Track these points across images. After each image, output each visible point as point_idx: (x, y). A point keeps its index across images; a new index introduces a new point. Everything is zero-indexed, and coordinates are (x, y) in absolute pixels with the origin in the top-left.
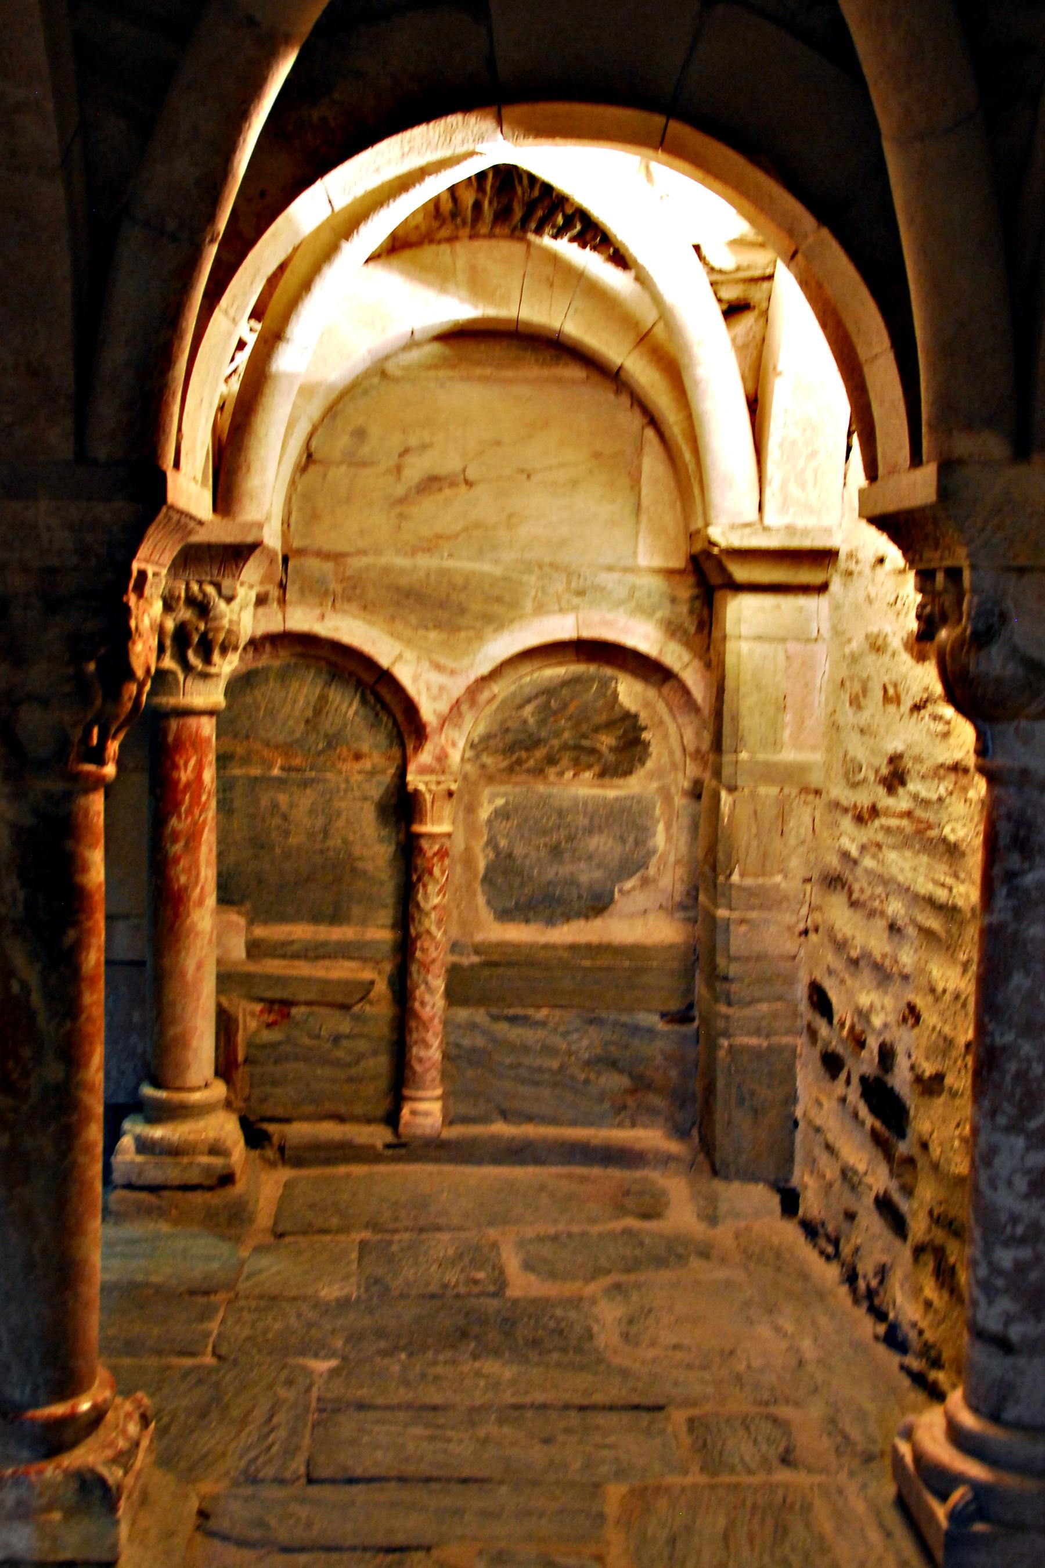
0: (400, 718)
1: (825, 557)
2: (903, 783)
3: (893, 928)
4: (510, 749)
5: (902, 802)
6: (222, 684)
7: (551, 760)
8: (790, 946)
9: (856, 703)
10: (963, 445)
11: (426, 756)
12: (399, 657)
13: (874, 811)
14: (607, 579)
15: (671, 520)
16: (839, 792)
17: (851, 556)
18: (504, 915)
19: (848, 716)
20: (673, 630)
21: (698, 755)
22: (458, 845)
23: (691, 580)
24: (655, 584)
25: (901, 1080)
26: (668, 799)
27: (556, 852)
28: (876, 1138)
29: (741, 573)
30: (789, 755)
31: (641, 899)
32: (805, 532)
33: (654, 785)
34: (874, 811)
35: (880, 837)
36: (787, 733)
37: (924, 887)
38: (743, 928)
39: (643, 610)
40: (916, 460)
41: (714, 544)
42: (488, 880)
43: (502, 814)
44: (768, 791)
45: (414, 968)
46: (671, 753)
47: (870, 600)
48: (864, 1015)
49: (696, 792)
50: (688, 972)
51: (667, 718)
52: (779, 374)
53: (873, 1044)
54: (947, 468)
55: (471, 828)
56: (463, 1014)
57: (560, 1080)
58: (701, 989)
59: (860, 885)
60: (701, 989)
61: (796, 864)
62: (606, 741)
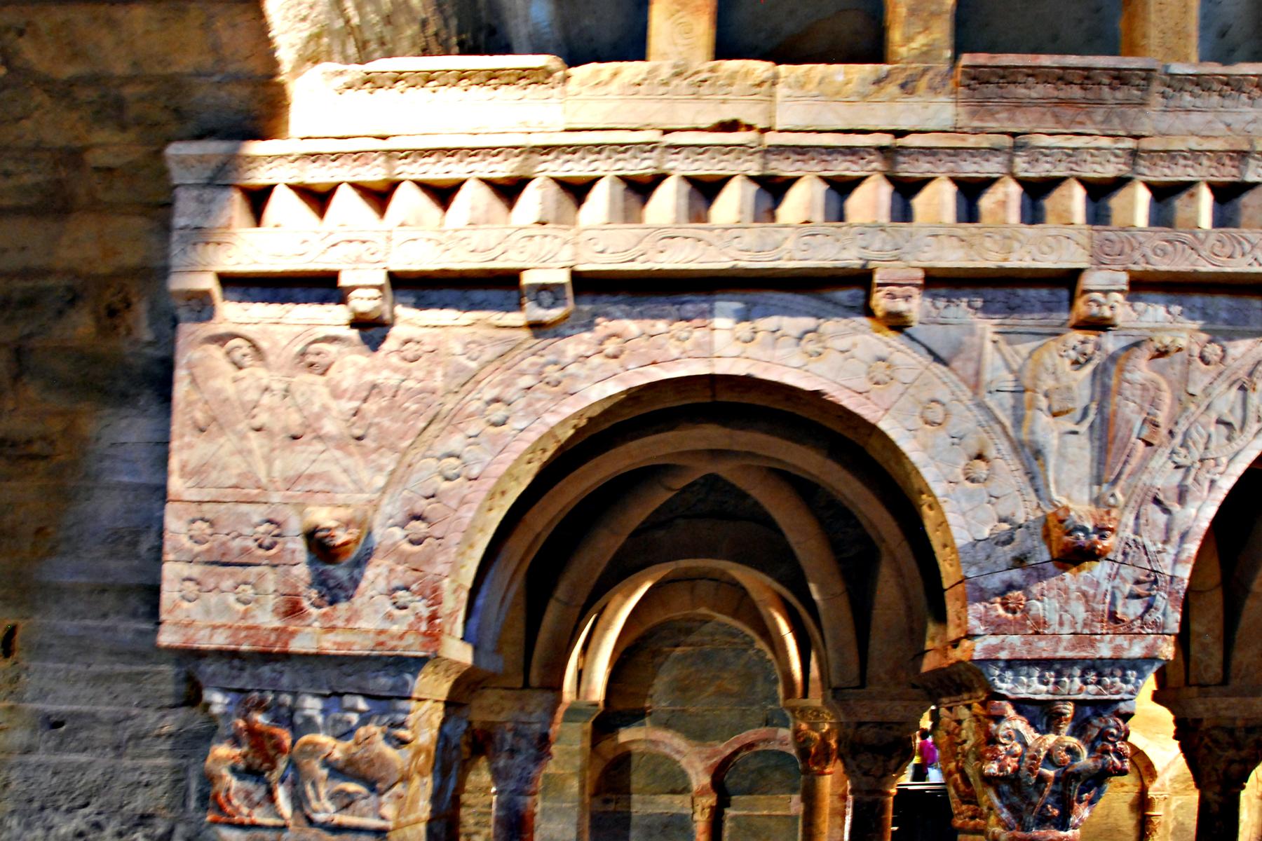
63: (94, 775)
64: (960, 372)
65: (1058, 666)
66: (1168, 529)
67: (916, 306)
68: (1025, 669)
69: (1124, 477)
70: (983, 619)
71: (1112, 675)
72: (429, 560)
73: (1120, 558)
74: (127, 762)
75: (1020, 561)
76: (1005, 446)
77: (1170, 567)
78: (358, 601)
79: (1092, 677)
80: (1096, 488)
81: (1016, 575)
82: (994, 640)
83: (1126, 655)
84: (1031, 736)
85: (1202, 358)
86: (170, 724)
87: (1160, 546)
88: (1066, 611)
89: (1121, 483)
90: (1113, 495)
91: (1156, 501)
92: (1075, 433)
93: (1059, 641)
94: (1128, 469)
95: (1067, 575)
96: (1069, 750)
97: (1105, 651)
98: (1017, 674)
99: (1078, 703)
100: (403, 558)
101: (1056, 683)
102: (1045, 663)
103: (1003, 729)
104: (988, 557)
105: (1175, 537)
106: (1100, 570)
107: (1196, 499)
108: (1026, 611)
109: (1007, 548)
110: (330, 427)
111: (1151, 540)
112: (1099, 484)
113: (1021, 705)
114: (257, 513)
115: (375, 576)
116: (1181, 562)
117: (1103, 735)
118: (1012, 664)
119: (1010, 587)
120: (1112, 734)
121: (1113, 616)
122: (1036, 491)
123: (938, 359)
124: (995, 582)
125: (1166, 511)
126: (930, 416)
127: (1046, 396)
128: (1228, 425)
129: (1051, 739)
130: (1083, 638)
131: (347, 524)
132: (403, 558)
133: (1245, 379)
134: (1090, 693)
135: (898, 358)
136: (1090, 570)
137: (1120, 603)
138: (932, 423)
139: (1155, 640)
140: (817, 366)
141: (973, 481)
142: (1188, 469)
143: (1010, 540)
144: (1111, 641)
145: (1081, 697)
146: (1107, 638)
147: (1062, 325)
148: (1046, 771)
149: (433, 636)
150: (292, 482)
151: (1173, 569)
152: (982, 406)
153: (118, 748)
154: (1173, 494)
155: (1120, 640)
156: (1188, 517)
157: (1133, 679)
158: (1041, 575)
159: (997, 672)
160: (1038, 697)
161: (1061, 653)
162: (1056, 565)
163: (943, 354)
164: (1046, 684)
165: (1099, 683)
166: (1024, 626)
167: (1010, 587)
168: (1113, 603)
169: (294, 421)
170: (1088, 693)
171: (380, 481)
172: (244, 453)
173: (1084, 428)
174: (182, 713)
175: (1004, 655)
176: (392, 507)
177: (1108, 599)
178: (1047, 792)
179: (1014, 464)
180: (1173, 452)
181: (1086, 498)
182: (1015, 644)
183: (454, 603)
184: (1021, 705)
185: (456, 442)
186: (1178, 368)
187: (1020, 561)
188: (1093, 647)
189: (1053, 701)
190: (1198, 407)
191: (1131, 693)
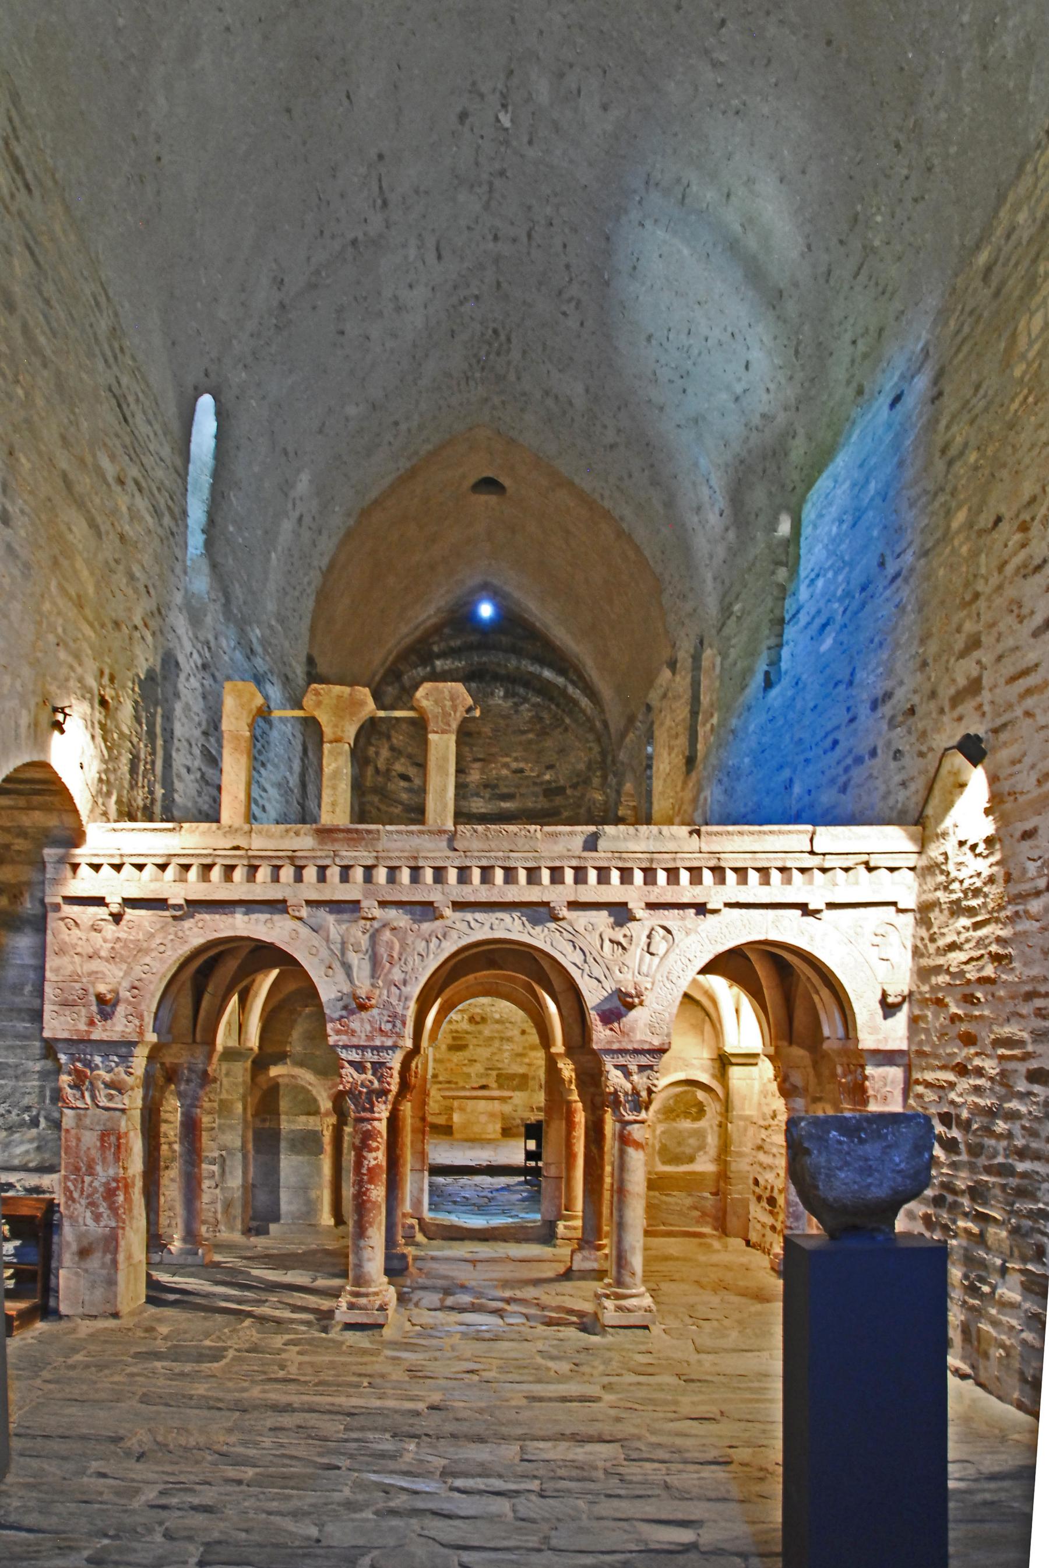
4: (665, 1113)
7: (678, 1116)
8: (748, 1168)
10: (780, 1043)
14: (695, 1062)
15: (713, 1043)
16: (762, 1123)
18: (664, 1163)
19: (763, 1101)
20: (714, 1076)
21: (721, 1114)
22: (650, 1142)
24: (708, 1063)
27: (679, 1144)
29: (734, 1060)
30: (747, 1113)
31: (705, 1158)
39: (705, 1071)
42: (659, 1153)
43: (663, 1133)
44: (742, 1123)
49: (720, 1125)
50: (718, 1181)
54: (777, 1048)
55: (654, 1137)
56: (652, 1193)
57: (681, 1213)
58: (722, 1184)
59: (766, 1147)
60: (722, 1184)
61: (750, 1145)
62: (694, 1110)
63: (8, 1090)
70: (333, 1029)
72: (139, 1004)
74: (21, 1084)
75: (345, 1008)
78: (115, 1019)
81: (344, 1013)
82: (337, 1038)
84: (356, 1075)
86: (38, 1066)
97: (378, 1043)
100: (130, 1003)
102: (357, 1047)
103: (343, 1071)
106: (375, 1012)
110: (103, 954)
111: (395, 1002)
113: (350, 1063)
114: (78, 986)
115: (121, 1010)
117: (382, 1075)
118: (345, 1047)
121: (381, 1030)
124: (336, 1015)
129: (363, 1076)
130: (369, 1038)
131: (110, 992)
132: (130, 1003)
134: (375, 1059)
143: (341, 999)
149: (141, 1033)
150: (90, 974)
153: (17, 1077)
158: (352, 1012)
167: (342, 1017)
169: (90, 951)
171: (121, 974)
172: (73, 963)
173: (367, 957)
174: (43, 1062)
176: (126, 984)
182: (344, 1039)
183: (149, 1020)
185: (147, 960)
187: (345, 1008)
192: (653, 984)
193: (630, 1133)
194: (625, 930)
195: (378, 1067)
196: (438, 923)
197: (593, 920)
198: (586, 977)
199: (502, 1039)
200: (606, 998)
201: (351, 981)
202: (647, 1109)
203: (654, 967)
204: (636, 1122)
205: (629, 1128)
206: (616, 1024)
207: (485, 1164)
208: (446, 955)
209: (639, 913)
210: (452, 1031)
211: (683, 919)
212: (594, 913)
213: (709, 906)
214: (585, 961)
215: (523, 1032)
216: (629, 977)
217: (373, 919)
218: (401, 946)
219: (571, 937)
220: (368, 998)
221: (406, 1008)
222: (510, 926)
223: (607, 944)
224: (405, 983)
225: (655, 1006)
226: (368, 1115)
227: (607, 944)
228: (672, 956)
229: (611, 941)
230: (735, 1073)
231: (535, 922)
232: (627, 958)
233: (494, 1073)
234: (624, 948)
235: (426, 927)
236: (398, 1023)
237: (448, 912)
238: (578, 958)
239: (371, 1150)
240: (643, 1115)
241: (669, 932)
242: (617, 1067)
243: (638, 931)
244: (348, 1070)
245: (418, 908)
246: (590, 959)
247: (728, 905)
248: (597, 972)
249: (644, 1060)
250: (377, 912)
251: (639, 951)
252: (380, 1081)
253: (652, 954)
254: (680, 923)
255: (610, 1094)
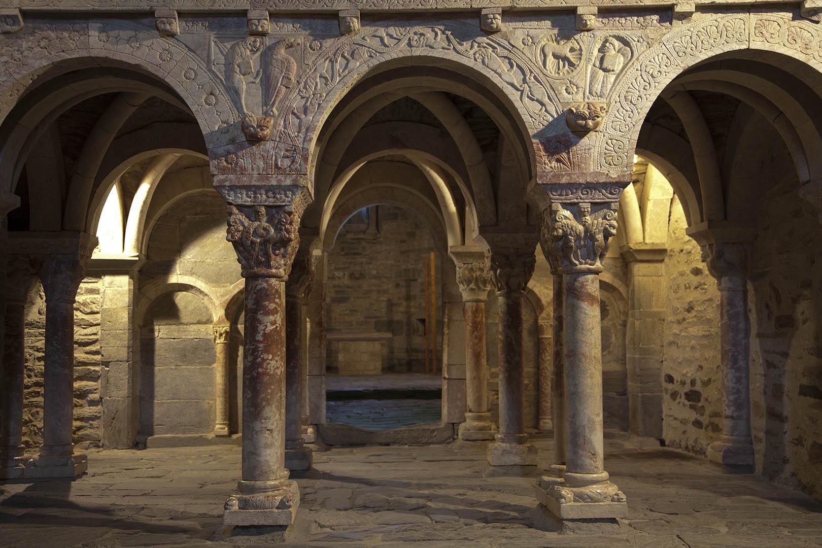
0: (534, 304)
1: (663, 251)
2: (693, 309)
3: (693, 348)
5: (693, 313)
6: (487, 292)
8: (658, 366)
9: (676, 292)
11: (544, 315)
12: (535, 285)
13: (684, 319)
17: (671, 250)
20: (616, 275)
23: (621, 260)
25: (698, 387)
26: (615, 327)
28: (691, 407)
29: (639, 257)
30: (655, 310)
32: (657, 244)
33: (611, 323)
34: (684, 319)
35: (686, 326)
36: (654, 303)
37: (701, 333)
38: (644, 360)
40: (702, 221)
41: (632, 249)
44: (649, 320)
45: (542, 378)
46: (616, 313)
47: (678, 262)
48: (685, 375)
51: (614, 302)
52: (649, 200)
53: (688, 381)
64: (200, 56)
65: (253, 189)
66: (300, 127)
67: (177, 26)
68: (238, 191)
69: (277, 103)
71: (280, 193)
73: (278, 139)
75: (232, 141)
76: (222, 89)
77: (302, 144)
79: (270, 194)
80: (265, 108)
81: (231, 147)
82: (222, 177)
83: (283, 184)
84: (246, 222)
85: (311, 48)
87: (296, 134)
88: (255, 164)
89: (275, 106)
90: (272, 111)
91: (293, 113)
92: (255, 83)
93: (252, 178)
94: (278, 99)
95: (254, 147)
96: (264, 229)
97: (274, 183)
98: (236, 193)
99: (267, 207)
101: (254, 197)
102: (248, 188)
104: (218, 139)
105: (304, 130)
106: (269, 145)
107: (312, 112)
108: (236, 164)
109: (226, 135)
111: (292, 131)
112: (266, 106)
113: (240, 207)
116: (307, 141)
117: (280, 221)
118: (232, 188)
119: (229, 153)
120: (283, 221)
122: (237, 109)
123: (190, 49)
124: (221, 151)
125: (298, 118)
126: (188, 75)
127: (239, 66)
128: (326, 78)
129: (257, 224)
133: (332, 56)
135: (173, 49)
136: (264, 145)
137: (279, 160)
138: (189, 79)
139: (297, 177)
140: (139, 53)
141: (209, 105)
142: (308, 99)
144: (276, 178)
145: (266, 204)
146: (274, 176)
147: (245, 34)
148: (254, 239)
151: (303, 144)
152: (210, 70)
154: (302, 110)
155: (280, 177)
156: (309, 121)
157: (290, 195)
159: (226, 192)
160: (247, 204)
161: (253, 183)
162: (248, 143)
163: (192, 47)
164: (250, 198)
165: (274, 197)
166: (235, 171)
168: (276, 160)
170: (269, 202)
173: (258, 80)
175: (227, 184)
177: (274, 159)
178: (257, 249)
179: (227, 97)
180: (299, 91)
181: (261, 112)
184: (240, 207)
186: (299, 52)
187: (232, 141)
188: (268, 180)
189: (254, 206)
190: (311, 70)
191: (290, 202)
192: (609, 105)
193: (583, 286)
194: (572, 43)
195: (276, 212)
196: (343, 39)
197: (532, 32)
198: (526, 100)
199: (379, 292)
200: (551, 124)
201: (239, 108)
202: (602, 256)
203: (609, 86)
204: (590, 272)
205: (582, 279)
206: (564, 155)
207: (372, 389)
208: (353, 79)
209: (592, 21)
210: (335, 286)
211: (643, 27)
212: (534, 24)
213: (678, 9)
214: (524, 81)
215: (397, 286)
216: (579, 97)
217: (263, 34)
218: (300, 67)
219: (506, 53)
220: (260, 126)
221: (307, 140)
222: (431, 41)
223: (550, 60)
224: (305, 111)
225: (611, 131)
226: (264, 271)
227: (550, 60)
228: (631, 73)
229: (555, 56)
230: (640, 271)
231: (462, 36)
232: (576, 76)
233: (373, 320)
234: (571, 64)
235: (328, 43)
236: (299, 159)
237: (356, 24)
238: (517, 80)
239: (268, 313)
240: (598, 264)
241: (626, 43)
242: (566, 206)
243: (590, 44)
244: (238, 217)
245: (319, 23)
246: (530, 79)
247: (702, 8)
248: (539, 92)
249: (598, 197)
250: (267, 25)
251: (590, 67)
252: (278, 230)
253: (605, 70)
254: (639, 33)
255: (558, 238)
